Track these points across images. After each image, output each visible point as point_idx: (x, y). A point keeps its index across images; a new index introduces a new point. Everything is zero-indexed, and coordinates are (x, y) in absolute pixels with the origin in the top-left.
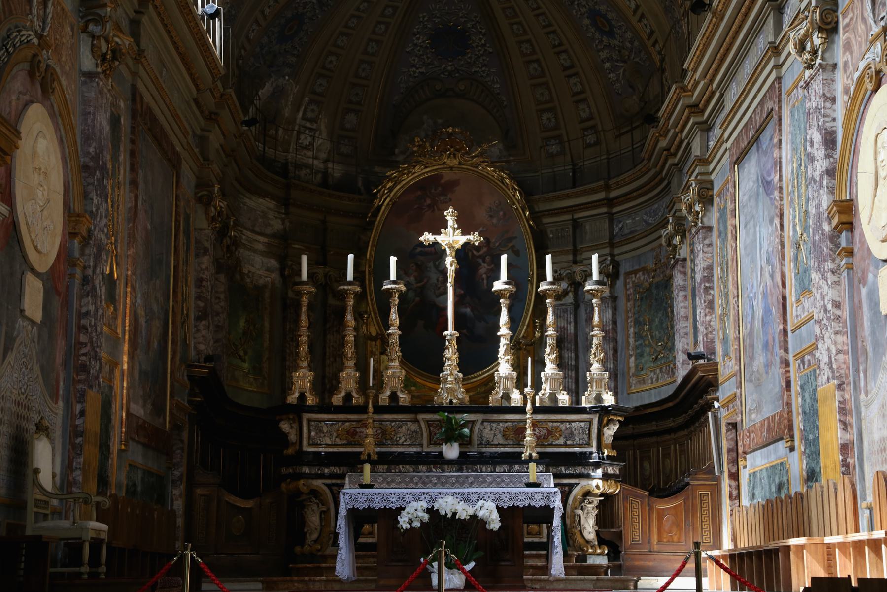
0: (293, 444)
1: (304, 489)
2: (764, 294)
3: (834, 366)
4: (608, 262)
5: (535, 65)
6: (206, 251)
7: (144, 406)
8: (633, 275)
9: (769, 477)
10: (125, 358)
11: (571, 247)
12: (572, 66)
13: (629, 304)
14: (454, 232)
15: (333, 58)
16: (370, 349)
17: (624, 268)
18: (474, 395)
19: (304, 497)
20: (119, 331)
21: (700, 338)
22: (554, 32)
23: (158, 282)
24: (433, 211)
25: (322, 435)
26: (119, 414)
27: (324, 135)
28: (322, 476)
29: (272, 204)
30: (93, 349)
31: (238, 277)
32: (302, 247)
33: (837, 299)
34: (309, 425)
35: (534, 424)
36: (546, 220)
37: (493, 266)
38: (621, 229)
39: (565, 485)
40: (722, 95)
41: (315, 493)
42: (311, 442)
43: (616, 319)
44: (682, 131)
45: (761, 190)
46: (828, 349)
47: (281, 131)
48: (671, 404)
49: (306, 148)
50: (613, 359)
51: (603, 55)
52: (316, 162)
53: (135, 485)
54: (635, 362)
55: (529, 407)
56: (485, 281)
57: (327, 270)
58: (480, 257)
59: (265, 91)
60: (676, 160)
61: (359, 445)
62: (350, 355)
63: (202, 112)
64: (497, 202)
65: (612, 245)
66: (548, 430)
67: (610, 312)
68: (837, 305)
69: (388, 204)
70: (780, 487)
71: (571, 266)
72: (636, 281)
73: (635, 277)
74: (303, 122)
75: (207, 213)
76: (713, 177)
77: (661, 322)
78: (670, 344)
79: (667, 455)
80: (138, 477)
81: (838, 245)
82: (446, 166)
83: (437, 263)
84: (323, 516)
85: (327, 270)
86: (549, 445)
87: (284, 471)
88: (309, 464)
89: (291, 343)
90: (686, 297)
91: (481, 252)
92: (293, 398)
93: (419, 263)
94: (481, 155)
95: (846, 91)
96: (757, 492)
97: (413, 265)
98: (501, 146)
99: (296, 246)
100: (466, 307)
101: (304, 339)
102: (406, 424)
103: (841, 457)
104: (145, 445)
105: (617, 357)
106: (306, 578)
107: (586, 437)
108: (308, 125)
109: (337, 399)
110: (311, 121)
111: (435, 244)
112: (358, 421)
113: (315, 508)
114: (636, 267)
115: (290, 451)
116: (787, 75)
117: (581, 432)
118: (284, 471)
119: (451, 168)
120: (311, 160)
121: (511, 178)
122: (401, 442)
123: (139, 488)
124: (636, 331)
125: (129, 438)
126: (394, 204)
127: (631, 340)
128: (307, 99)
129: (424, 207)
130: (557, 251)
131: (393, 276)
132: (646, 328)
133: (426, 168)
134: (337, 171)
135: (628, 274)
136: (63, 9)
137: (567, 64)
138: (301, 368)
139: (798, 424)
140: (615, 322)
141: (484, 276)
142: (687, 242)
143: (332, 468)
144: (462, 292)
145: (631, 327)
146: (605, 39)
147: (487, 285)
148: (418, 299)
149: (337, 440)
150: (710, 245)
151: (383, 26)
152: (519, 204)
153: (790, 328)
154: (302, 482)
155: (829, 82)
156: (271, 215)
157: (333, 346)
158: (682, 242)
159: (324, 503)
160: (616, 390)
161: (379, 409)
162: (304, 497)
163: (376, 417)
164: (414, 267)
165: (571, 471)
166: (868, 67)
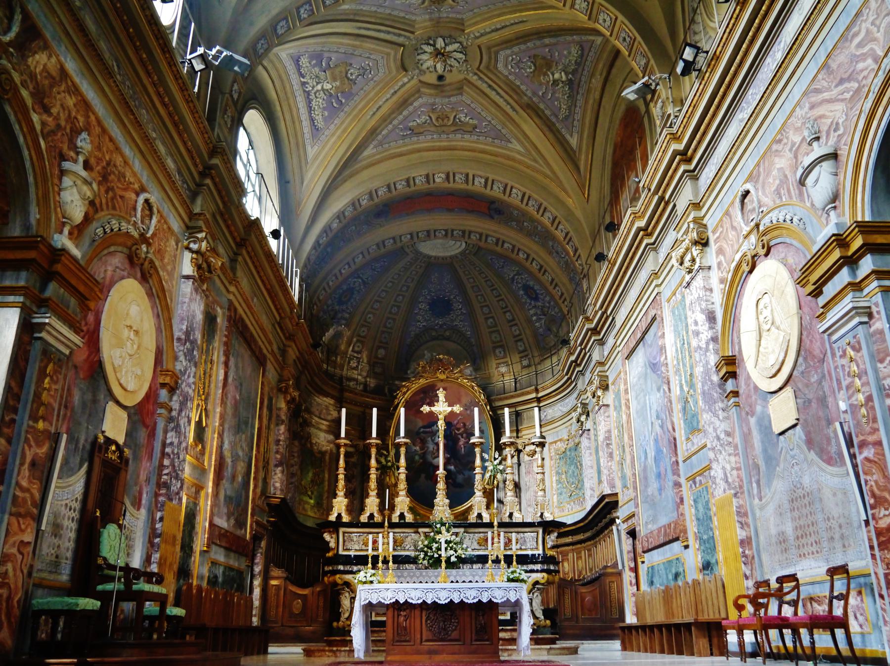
0: (333, 549)
1: (339, 581)
2: (656, 441)
3: (730, 480)
5: (491, 320)
6: (283, 421)
7: (228, 520)
9: (666, 569)
10: (211, 484)
12: (513, 320)
15: (371, 316)
17: (548, 440)
19: (339, 587)
20: (206, 464)
21: (604, 478)
22: (502, 300)
23: (244, 436)
26: (202, 524)
27: (365, 361)
29: (332, 402)
30: (175, 471)
31: (309, 445)
33: (729, 430)
34: (344, 536)
40: (613, 318)
44: (586, 347)
45: (649, 370)
46: (723, 468)
47: (339, 359)
48: (582, 524)
49: (356, 368)
51: (532, 312)
52: (360, 377)
53: (216, 577)
59: (331, 332)
60: (581, 369)
63: (284, 334)
68: (728, 434)
70: (676, 576)
75: (285, 398)
76: (607, 374)
77: (573, 472)
78: (580, 486)
79: (579, 558)
80: (220, 571)
81: (725, 391)
87: (326, 569)
88: (344, 564)
90: (591, 454)
92: (333, 518)
94: (460, 372)
95: (722, 281)
96: (656, 580)
98: (471, 369)
103: (741, 550)
104: (226, 548)
106: (335, 649)
107: (535, 544)
109: (364, 518)
110: (358, 352)
111: (431, 413)
113: (347, 594)
115: (330, 554)
116: (665, 291)
118: (326, 569)
119: (442, 380)
121: (478, 386)
123: (220, 580)
125: (211, 542)
127: (554, 485)
128: (355, 339)
132: (563, 476)
134: (372, 382)
136: (169, 228)
137: (510, 318)
139: (692, 528)
142: (590, 418)
146: (533, 302)
150: (608, 417)
151: (401, 297)
153: (680, 460)
154: (338, 576)
155: (706, 279)
156: (331, 408)
158: (587, 419)
161: (392, 526)
162: (339, 587)
166: (744, 255)
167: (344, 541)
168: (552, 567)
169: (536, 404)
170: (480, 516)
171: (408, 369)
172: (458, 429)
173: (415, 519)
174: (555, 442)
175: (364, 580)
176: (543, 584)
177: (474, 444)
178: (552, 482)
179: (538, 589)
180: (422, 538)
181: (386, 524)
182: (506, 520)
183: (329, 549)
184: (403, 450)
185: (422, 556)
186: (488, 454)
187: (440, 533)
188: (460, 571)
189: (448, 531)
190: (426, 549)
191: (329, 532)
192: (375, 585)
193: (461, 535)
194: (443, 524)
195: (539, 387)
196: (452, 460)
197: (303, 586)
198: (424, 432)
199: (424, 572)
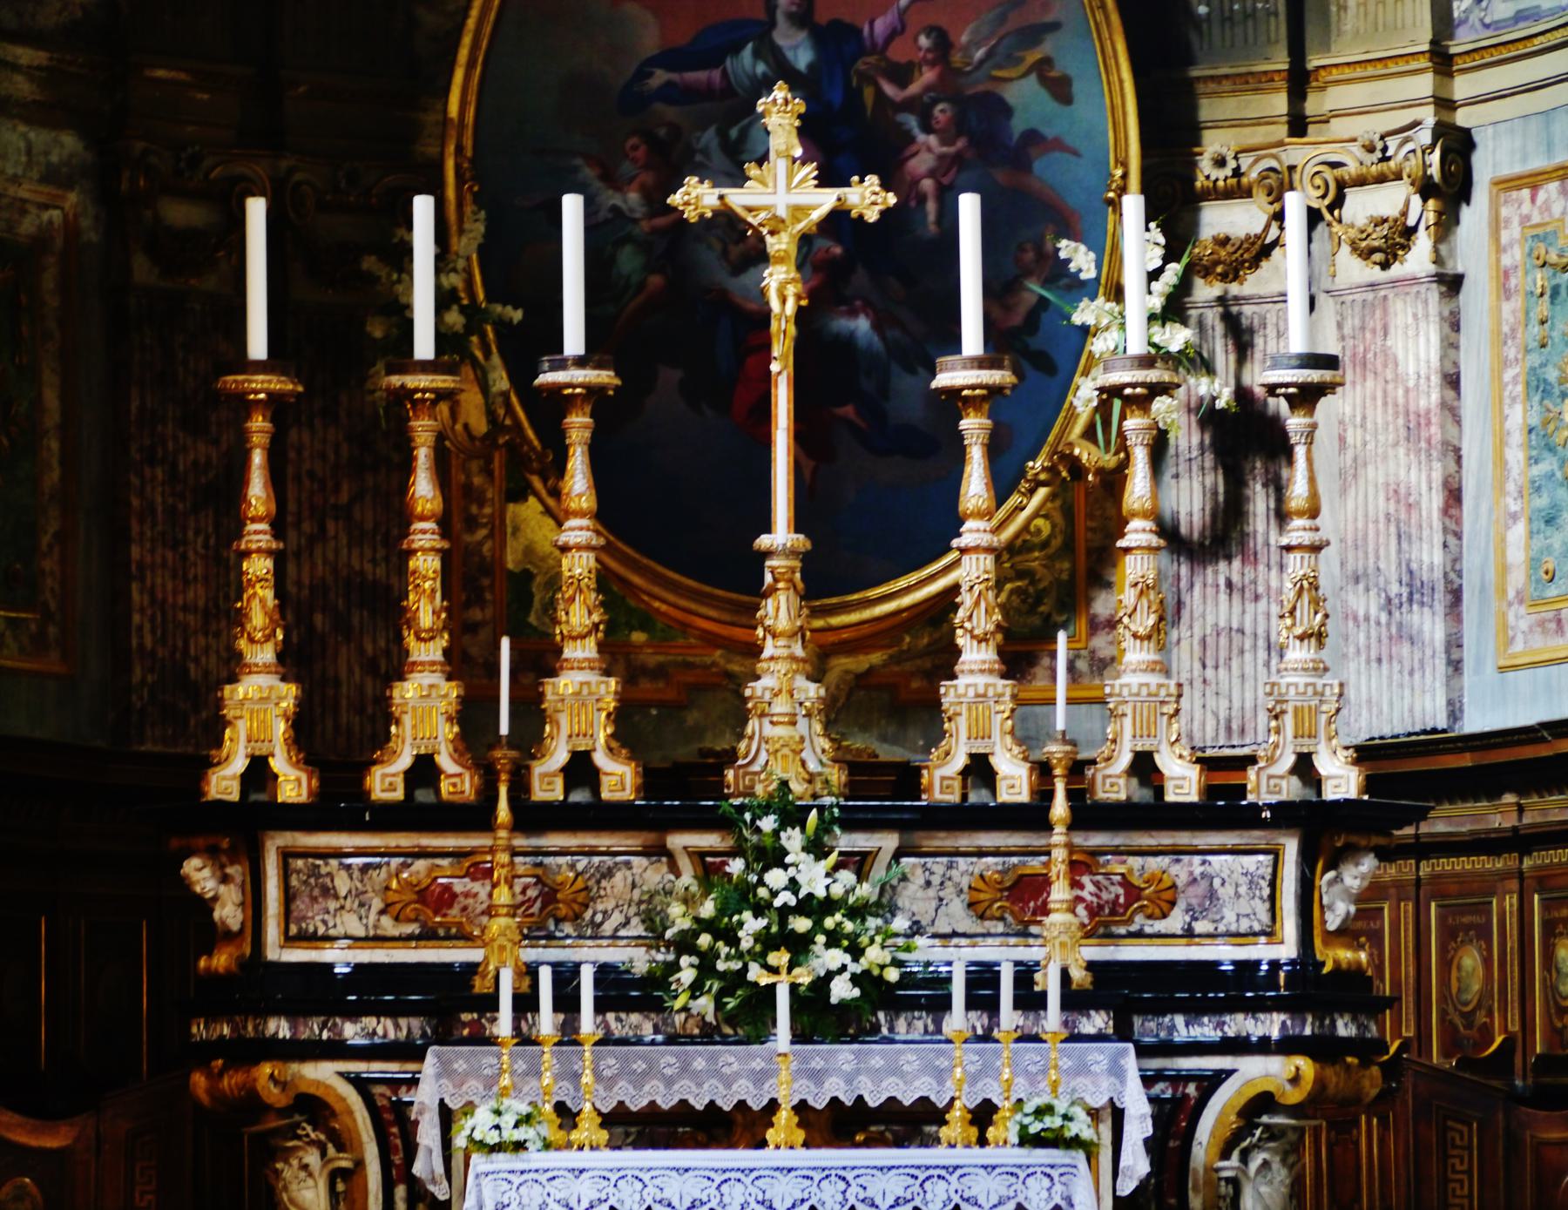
0: (229, 936)
1: (273, 1095)
4: (1424, 136)
8: (1526, 193)
11: (1281, 62)
13: (1507, 308)
14: (790, 176)
16: (462, 478)
17: (1485, 166)
18: (885, 665)
25: (332, 905)
28: (337, 1050)
32: (182, 76)
34: (286, 873)
35: (1081, 865)
37: (961, 143)
39: (1180, 1079)
41: (314, 1108)
42: (293, 929)
43: (1456, 364)
50: (1445, 530)
54: (1528, 547)
55: (1060, 808)
56: (931, 207)
57: (284, 164)
58: (909, 105)
61: (463, 937)
62: (426, 619)
65: (1442, 61)
66: (1126, 883)
67: (1435, 339)
71: (1281, 144)
72: (1536, 219)
73: (1533, 200)
83: (734, 133)
84: (340, 1187)
85: (284, 164)
86: (1131, 935)
87: (199, 1030)
88: (295, 1013)
89: (147, 471)
91: (914, 88)
92: (224, 783)
93: (662, 132)
97: (633, 141)
99: (161, 73)
100: (853, 313)
101: (259, 566)
102: (628, 865)
105: (1459, 521)
107: (1262, 910)
111: (727, 222)
112: (458, 854)
113: (312, 1158)
114: (1537, 163)
115: (221, 960)
117: (1243, 890)
118: (199, 1030)
122: (608, 928)
124: (1534, 420)
127: (1516, 456)
130: (1227, 77)
131: (574, 340)
135: (1507, 184)
138: (251, 670)
140: (1452, 381)
141: (927, 184)
143: (370, 1022)
144: (838, 250)
145: (1514, 400)
147: (939, 221)
148: (655, 280)
149: (386, 921)
154: (267, 1069)
157: (311, 474)
159: (342, 1141)
160: (1454, 656)
161: (533, 817)
163: (520, 842)
164: (640, 153)
165: (1206, 1031)
167: (289, 897)
168: (1345, 1028)
170: (980, 770)
172: (902, 75)
173: (650, 782)
174: (1533, 181)
175: (492, 1138)
176: (1294, 1111)
177: (953, 393)
178: (1502, 440)
179: (1272, 1133)
180: (687, 879)
181: (503, 812)
182: (1114, 784)
183: (215, 936)
184: (579, 426)
185: (687, 975)
186: (1096, 247)
187: (777, 857)
188: (876, 1055)
189: (817, 849)
190: (705, 940)
191: (212, 854)
192: (535, 1158)
193: (878, 872)
194: (792, 816)
196: (860, 279)
197: (43, 1112)
198: (669, 93)
199: (700, 1057)
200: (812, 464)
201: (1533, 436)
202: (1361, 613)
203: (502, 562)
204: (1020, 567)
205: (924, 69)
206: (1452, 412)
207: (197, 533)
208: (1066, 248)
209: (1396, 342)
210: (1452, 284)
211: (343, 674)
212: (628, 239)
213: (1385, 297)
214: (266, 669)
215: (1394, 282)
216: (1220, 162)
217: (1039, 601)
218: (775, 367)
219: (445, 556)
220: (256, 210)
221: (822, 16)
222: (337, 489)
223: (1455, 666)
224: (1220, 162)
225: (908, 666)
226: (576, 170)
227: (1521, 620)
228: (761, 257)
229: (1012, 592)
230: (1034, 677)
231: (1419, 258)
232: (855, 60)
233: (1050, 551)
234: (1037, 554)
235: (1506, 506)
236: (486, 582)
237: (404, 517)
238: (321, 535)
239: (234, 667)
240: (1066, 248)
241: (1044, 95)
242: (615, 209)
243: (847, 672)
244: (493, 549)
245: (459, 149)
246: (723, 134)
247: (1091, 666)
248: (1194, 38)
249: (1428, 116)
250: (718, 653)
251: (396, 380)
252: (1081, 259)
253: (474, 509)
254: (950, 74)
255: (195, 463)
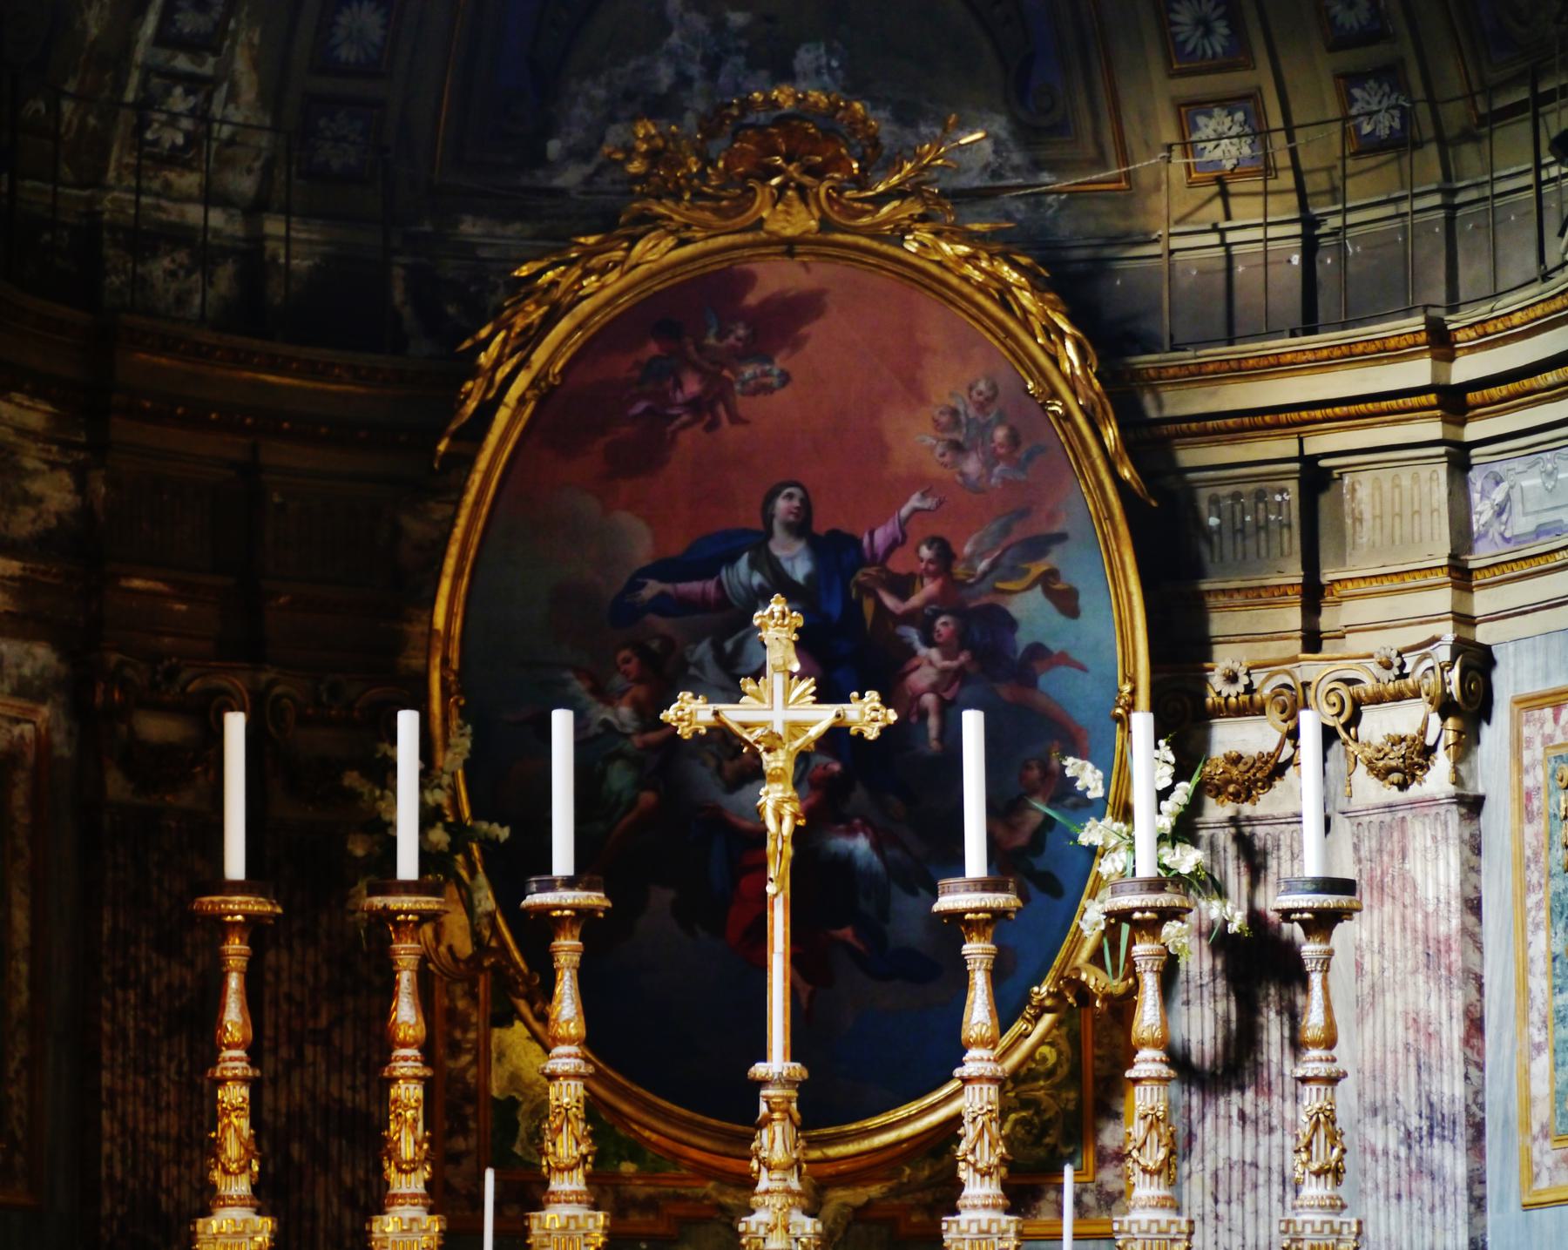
4: (1444, 653)
8: (1548, 712)
11: (1294, 574)
13: (1529, 830)
14: (787, 691)
16: (446, 1002)
17: (1506, 684)
18: (885, 1197)
24: (713, 425)
27: (248, 94)
29: (35, 418)
32: (160, 587)
36: (1189, 456)
37: (963, 657)
38: (1500, 511)
43: (1477, 889)
47: (67, 107)
49: (175, 159)
50: (1467, 1061)
52: (217, 218)
54: (1553, 1079)
56: (933, 722)
57: (264, 677)
58: (909, 618)
62: (407, 1150)
64: (982, 386)
65: (1461, 575)
69: (522, 401)
71: (1294, 660)
72: (1559, 739)
73: (1556, 719)
74: (162, 55)
82: (763, 235)
85: (264, 677)
89: (119, 994)
91: (915, 601)
93: (655, 645)
97: (625, 653)
99: (137, 583)
100: (852, 832)
101: (234, 1095)
105: (1481, 1052)
108: (182, 63)
110: (196, 46)
111: (722, 738)
119: (790, 247)
120: (194, 213)
124: (1558, 948)
126: (545, 393)
127: (1539, 984)
129: (675, 412)
130: (1238, 590)
131: (563, 860)
133: (682, 243)
135: (1529, 703)
138: (226, 1202)
140: (1473, 906)
141: (929, 700)
144: (836, 767)
145: (1537, 926)
147: (941, 737)
148: (648, 797)
152: (1075, 393)
160: (1477, 1193)
164: (632, 667)
169: (1432, 429)
171: (548, 129)
172: (903, 587)
177: (956, 916)
178: (1525, 968)
184: (567, 950)
186: (1104, 765)
195: (1454, 322)
196: (860, 795)
198: (663, 605)
200: (809, 988)
201: (1558, 965)
202: (1380, 1147)
203: (486, 1088)
204: (1024, 1096)
205: (926, 581)
206: (1473, 938)
207: (170, 1058)
208: (1072, 765)
209: (1415, 865)
210: (1472, 806)
211: (321, 1206)
212: (620, 755)
213: (1403, 819)
214: (241, 1202)
215: (1412, 804)
216: (1232, 678)
217: (1044, 1132)
218: (771, 889)
219: (428, 1085)
220: (235, 726)
221: (821, 526)
222: (315, 1014)
223: (1478, 1203)
224: (1232, 678)
225: (909, 1199)
226: (565, 683)
227: (1545, 1154)
228: (756, 773)
229: (1016, 1122)
230: (1039, 1212)
231: (1438, 778)
232: (854, 573)
233: (1057, 1079)
234: (1042, 1083)
235: (1530, 1036)
236: (469, 1110)
237: (384, 1042)
238: (299, 1061)
239: (207, 1200)
240: (1072, 765)
241: (1049, 606)
242: (606, 724)
243: (845, 1205)
244: (477, 1077)
245: (445, 662)
246: (717, 648)
247: (1098, 1200)
248: (1204, 549)
249: (1447, 632)
250: (711, 1184)
251: (378, 902)
252: (1088, 777)
253: (458, 1034)
254: (952, 586)
255: (169, 986)
